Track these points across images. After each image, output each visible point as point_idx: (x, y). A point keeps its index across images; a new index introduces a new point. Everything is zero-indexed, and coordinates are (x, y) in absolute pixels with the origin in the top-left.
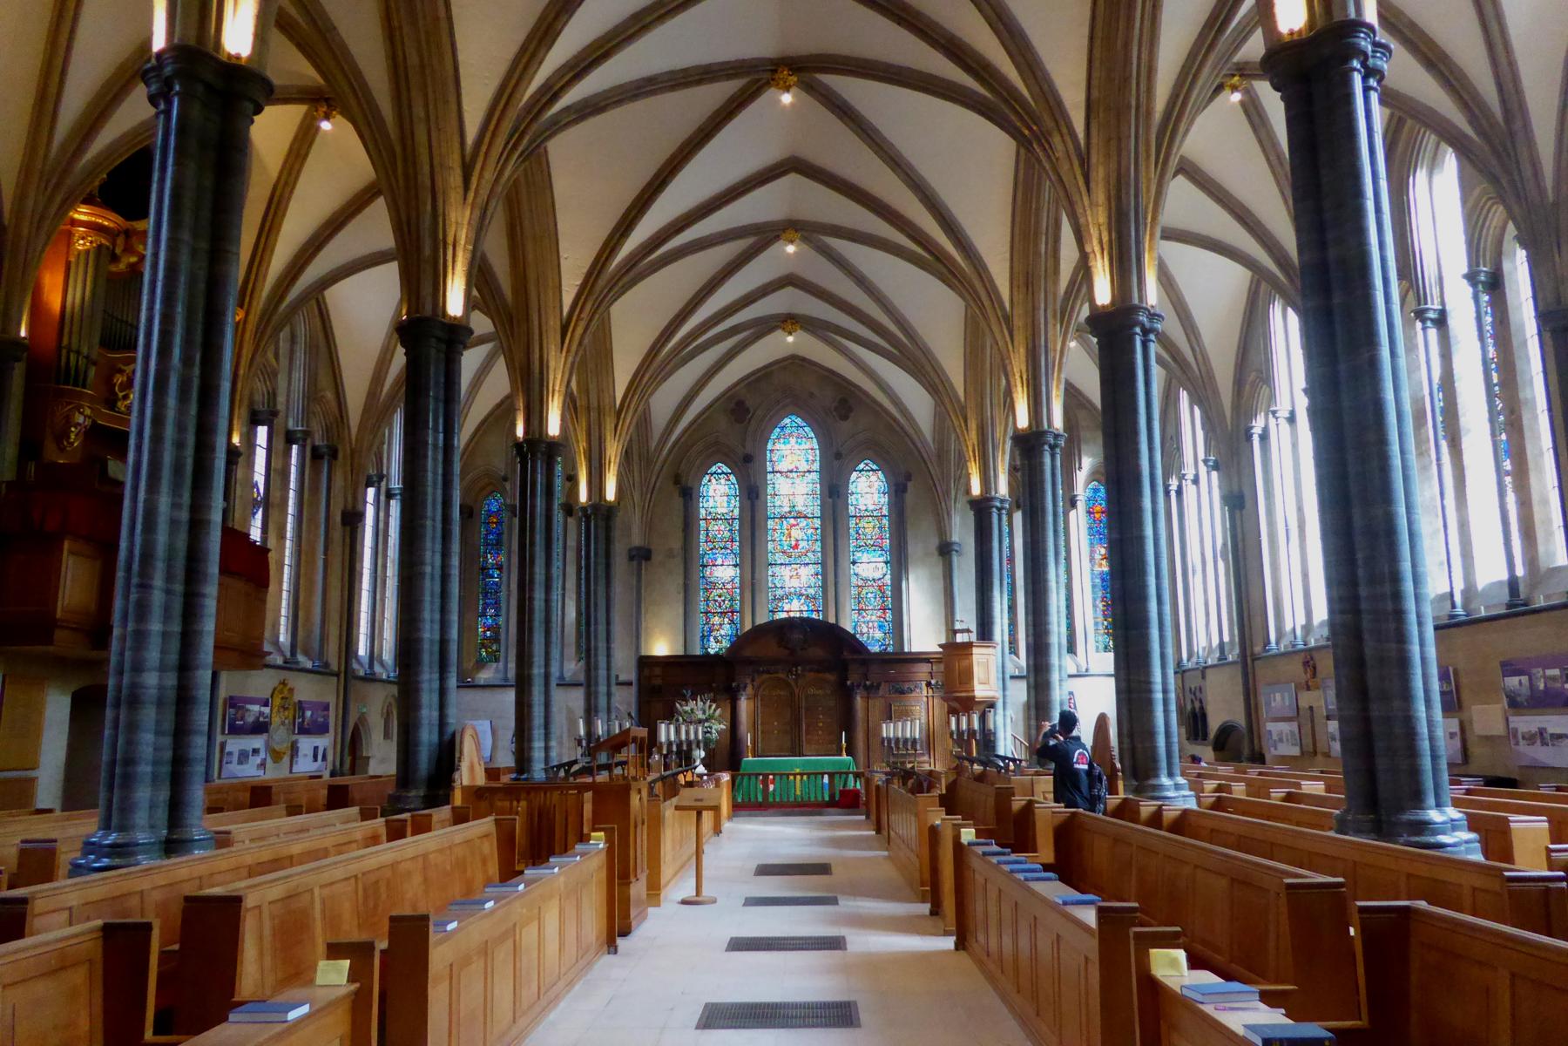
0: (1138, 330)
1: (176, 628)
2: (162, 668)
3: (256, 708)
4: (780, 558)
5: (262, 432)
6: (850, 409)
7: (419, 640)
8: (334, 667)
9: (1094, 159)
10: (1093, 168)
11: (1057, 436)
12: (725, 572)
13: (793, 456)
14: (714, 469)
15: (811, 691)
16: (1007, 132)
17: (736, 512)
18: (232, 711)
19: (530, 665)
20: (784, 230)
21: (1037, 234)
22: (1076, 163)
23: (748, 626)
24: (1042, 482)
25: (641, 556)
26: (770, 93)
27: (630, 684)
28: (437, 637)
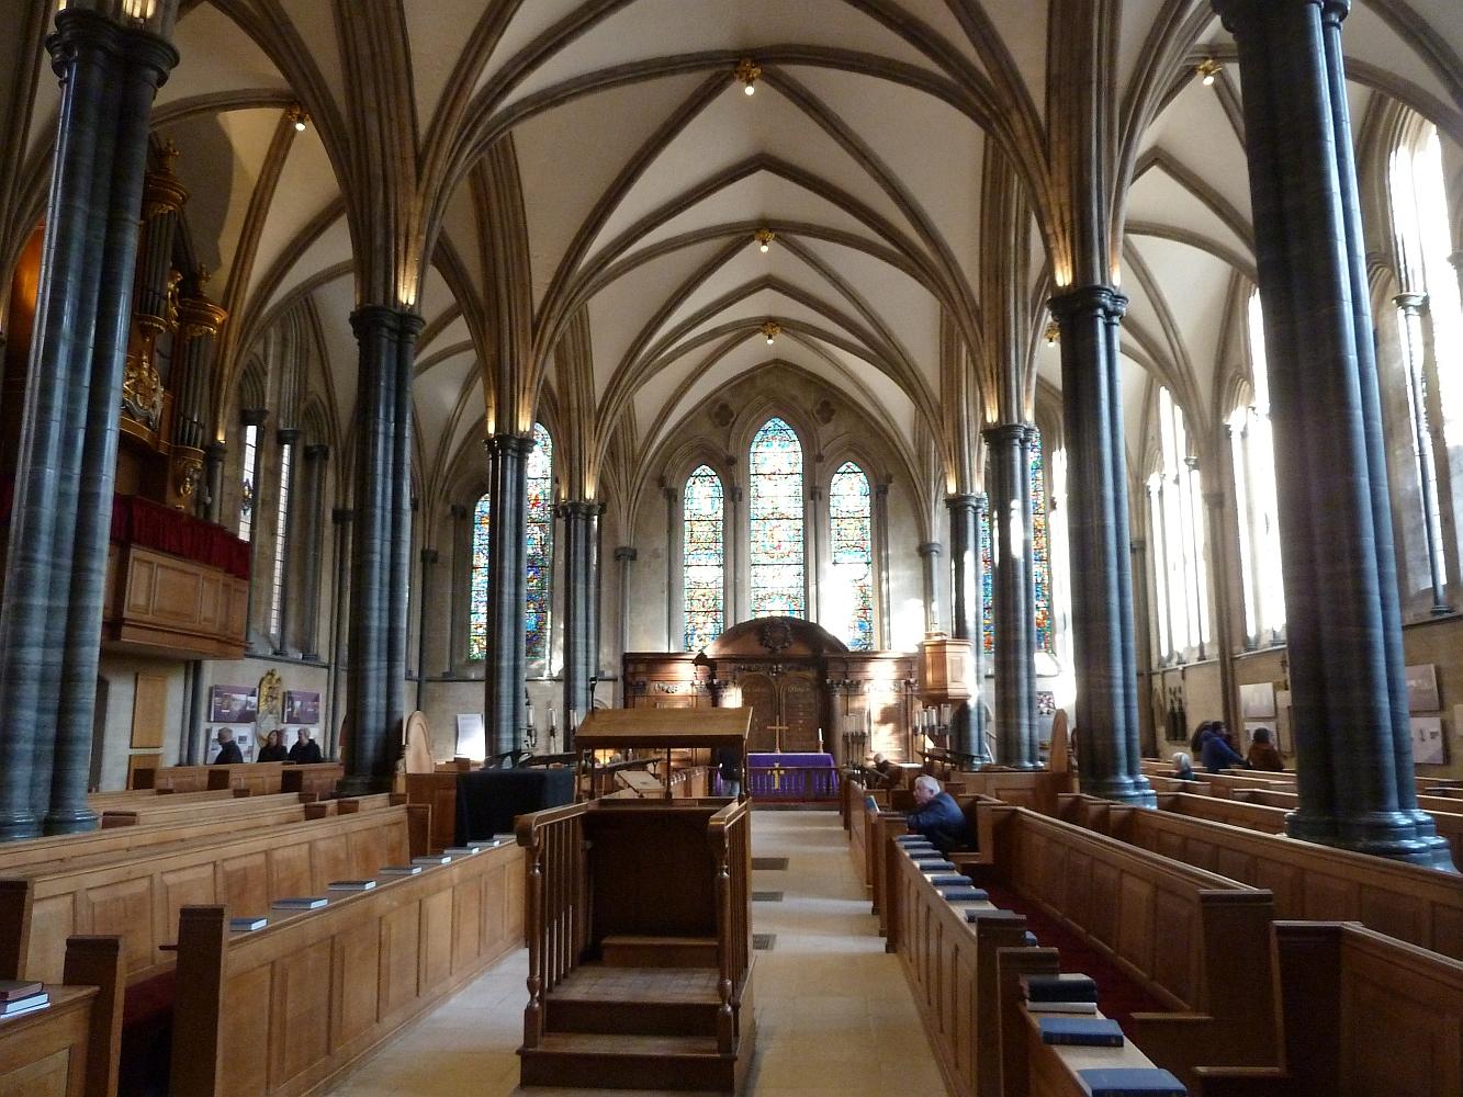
0: (1100, 312)
1: (62, 602)
2: (47, 644)
3: (243, 697)
4: (764, 559)
5: (251, 432)
6: (832, 412)
8: (325, 658)
9: (1054, 137)
10: (1054, 146)
11: (1027, 431)
13: (776, 457)
14: (698, 471)
15: (793, 689)
16: (968, 114)
17: (720, 515)
18: (216, 700)
19: (499, 657)
20: (758, 231)
21: (1006, 226)
22: (1036, 141)
23: (731, 625)
24: (1012, 476)
26: (735, 85)
27: (614, 680)
28: (385, 625)
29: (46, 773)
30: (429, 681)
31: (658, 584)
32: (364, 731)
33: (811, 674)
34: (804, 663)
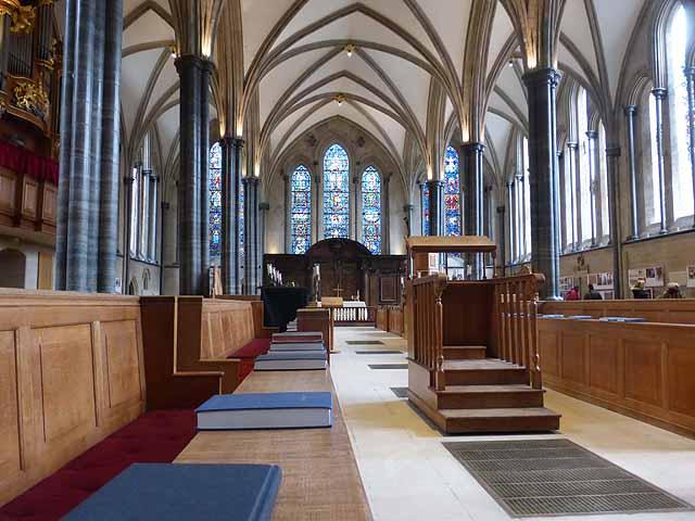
7: (191, 222)
11: (482, 146)
12: (300, 216)
13: (336, 161)
17: (309, 189)
19: (229, 248)
23: (314, 242)
25: (266, 207)
29: (94, 272)
30: (166, 267)
31: (278, 222)
32: (191, 274)
33: (354, 265)
34: (350, 261)
